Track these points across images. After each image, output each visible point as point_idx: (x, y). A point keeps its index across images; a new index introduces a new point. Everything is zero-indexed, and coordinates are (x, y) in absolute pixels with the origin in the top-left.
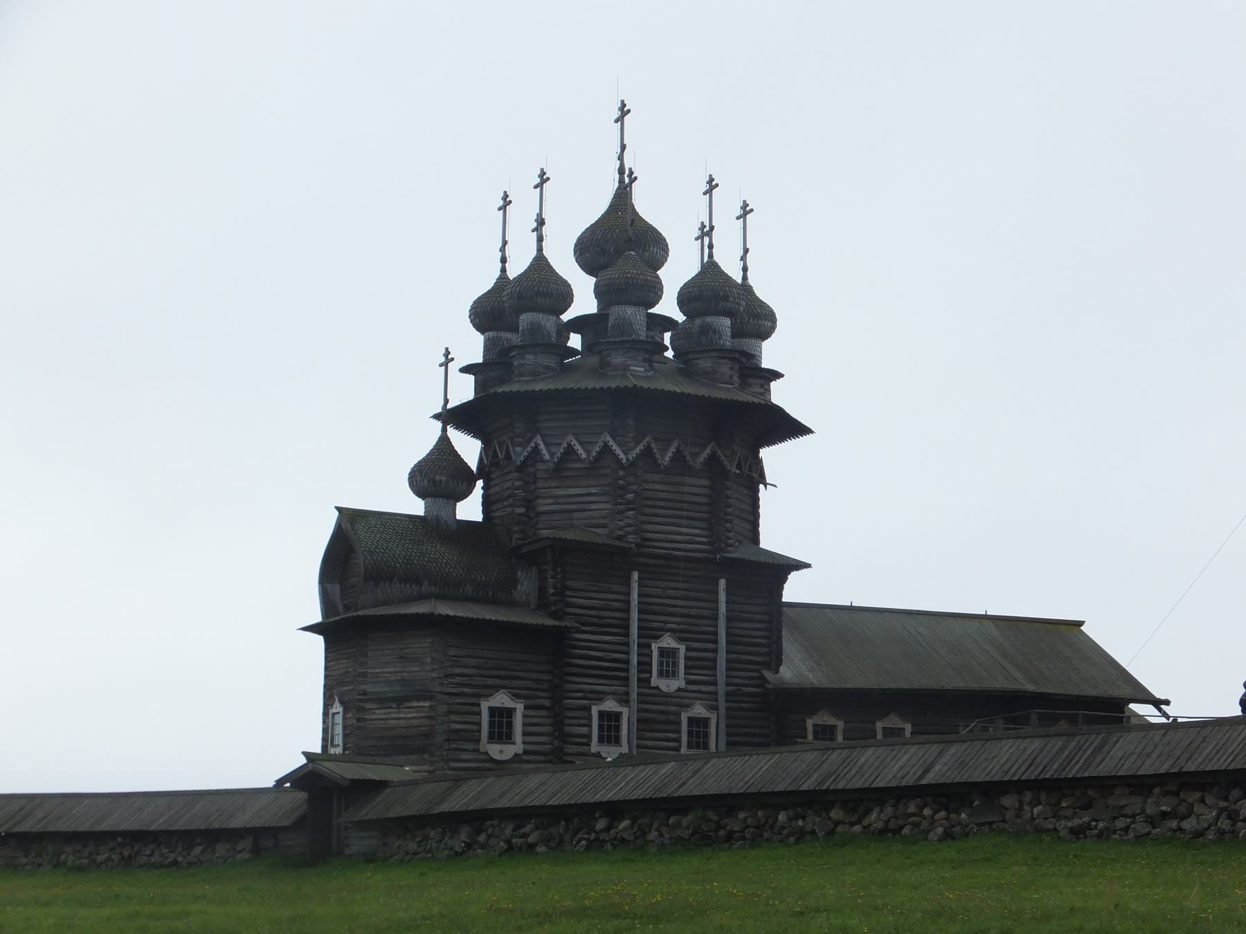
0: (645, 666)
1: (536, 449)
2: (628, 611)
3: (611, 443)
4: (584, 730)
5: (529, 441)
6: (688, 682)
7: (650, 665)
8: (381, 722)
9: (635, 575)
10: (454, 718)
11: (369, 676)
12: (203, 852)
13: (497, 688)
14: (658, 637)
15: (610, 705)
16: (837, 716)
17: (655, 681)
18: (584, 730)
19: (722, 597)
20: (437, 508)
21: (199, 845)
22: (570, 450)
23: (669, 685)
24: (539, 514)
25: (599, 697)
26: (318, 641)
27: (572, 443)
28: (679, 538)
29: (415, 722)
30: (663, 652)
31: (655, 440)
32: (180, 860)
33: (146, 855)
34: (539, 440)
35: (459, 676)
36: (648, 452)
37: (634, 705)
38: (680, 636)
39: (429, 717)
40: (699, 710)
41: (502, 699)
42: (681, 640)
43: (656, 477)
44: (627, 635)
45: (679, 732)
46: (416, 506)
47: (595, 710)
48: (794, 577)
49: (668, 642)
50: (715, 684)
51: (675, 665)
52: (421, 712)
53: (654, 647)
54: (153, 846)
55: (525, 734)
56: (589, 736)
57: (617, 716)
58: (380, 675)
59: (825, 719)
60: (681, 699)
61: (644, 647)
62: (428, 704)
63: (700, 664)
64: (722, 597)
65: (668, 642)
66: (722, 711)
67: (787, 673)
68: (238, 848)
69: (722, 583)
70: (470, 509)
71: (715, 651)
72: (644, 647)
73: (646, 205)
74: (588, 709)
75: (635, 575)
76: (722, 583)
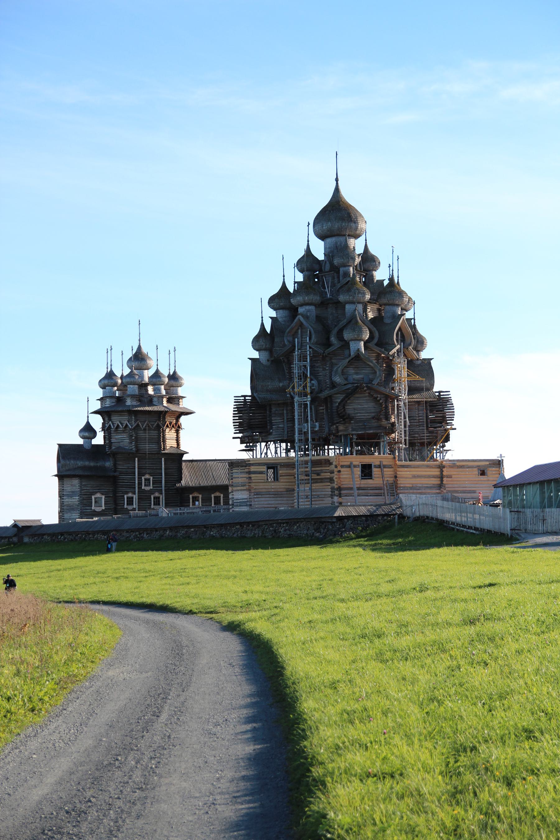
0: (140, 484)
1: (110, 425)
2: (135, 469)
4: (123, 502)
6: (153, 487)
7: (142, 483)
9: (136, 459)
13: (96, 492)
14: (144, 475)
15: (130, 495)
16: (200, 494)
17: (143, 487)
18: (123, 502)
19: (163, 463)
22: (118, 425)
23: (147, 488)
24: (112, 443)
25: (127, 493)
26: (57, 478)
29: (75, 503)
30: (145, 479)
31: (140, 422)
34: (110, 422)
36: (138, 425)
37: (137, 494)
38: (150, 474)
40: (157, 494)
41: (98, 495)
42: (151, 476)
43: (142, 432)
44: (135, 475)
45: (151, 501)
46: (80, 441)
47: (125, 496)
48: (185, 455)
49: (147, 476)
50: (162, 487)
51: (150, 483)
53: (143, 478)
55: (105, 504)
56: (124, 504)
57: (132, 498)
59: (196, 495)
60: (151, 492)
61: (140, 479)
63: (157, 482)
64: (163, 463)
65: (147, 476)
66: (164, 494)
67: (183, 482)
69: (163, 459)
70: (99, 440)
71: (162, 478)
72: (140, 479)
73: (145, 350)
74: (124, 496)
75: (136, 459)
76: (163, 459)
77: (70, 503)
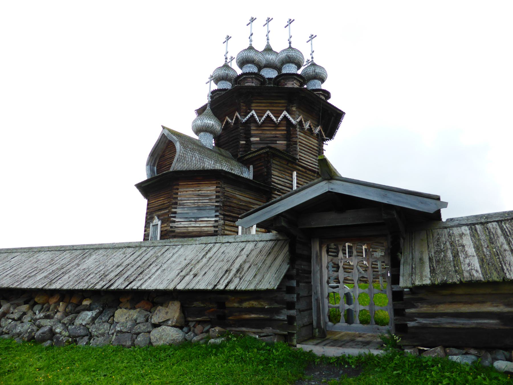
3: (288, 115)
5: (249, 113)
8: (185, 228)
9: (295, 174)
10: (226, 228)
11: (178, 204)
12: (93, 319)
20: (206, 137)
21: (89, 308)
27: (269, 115)
28: (310, 161)
29: (206, 229)
32: (58, 330)
33: (13, 319)
34: (253, 112)
35: (228, 206)
39: (214, 227)
52: (210, 224)
54: (24, 308)
58: (185, 204)
62: (214, 219)
68: (155, 319)
75: (295, 174)
77: (190, 229)
